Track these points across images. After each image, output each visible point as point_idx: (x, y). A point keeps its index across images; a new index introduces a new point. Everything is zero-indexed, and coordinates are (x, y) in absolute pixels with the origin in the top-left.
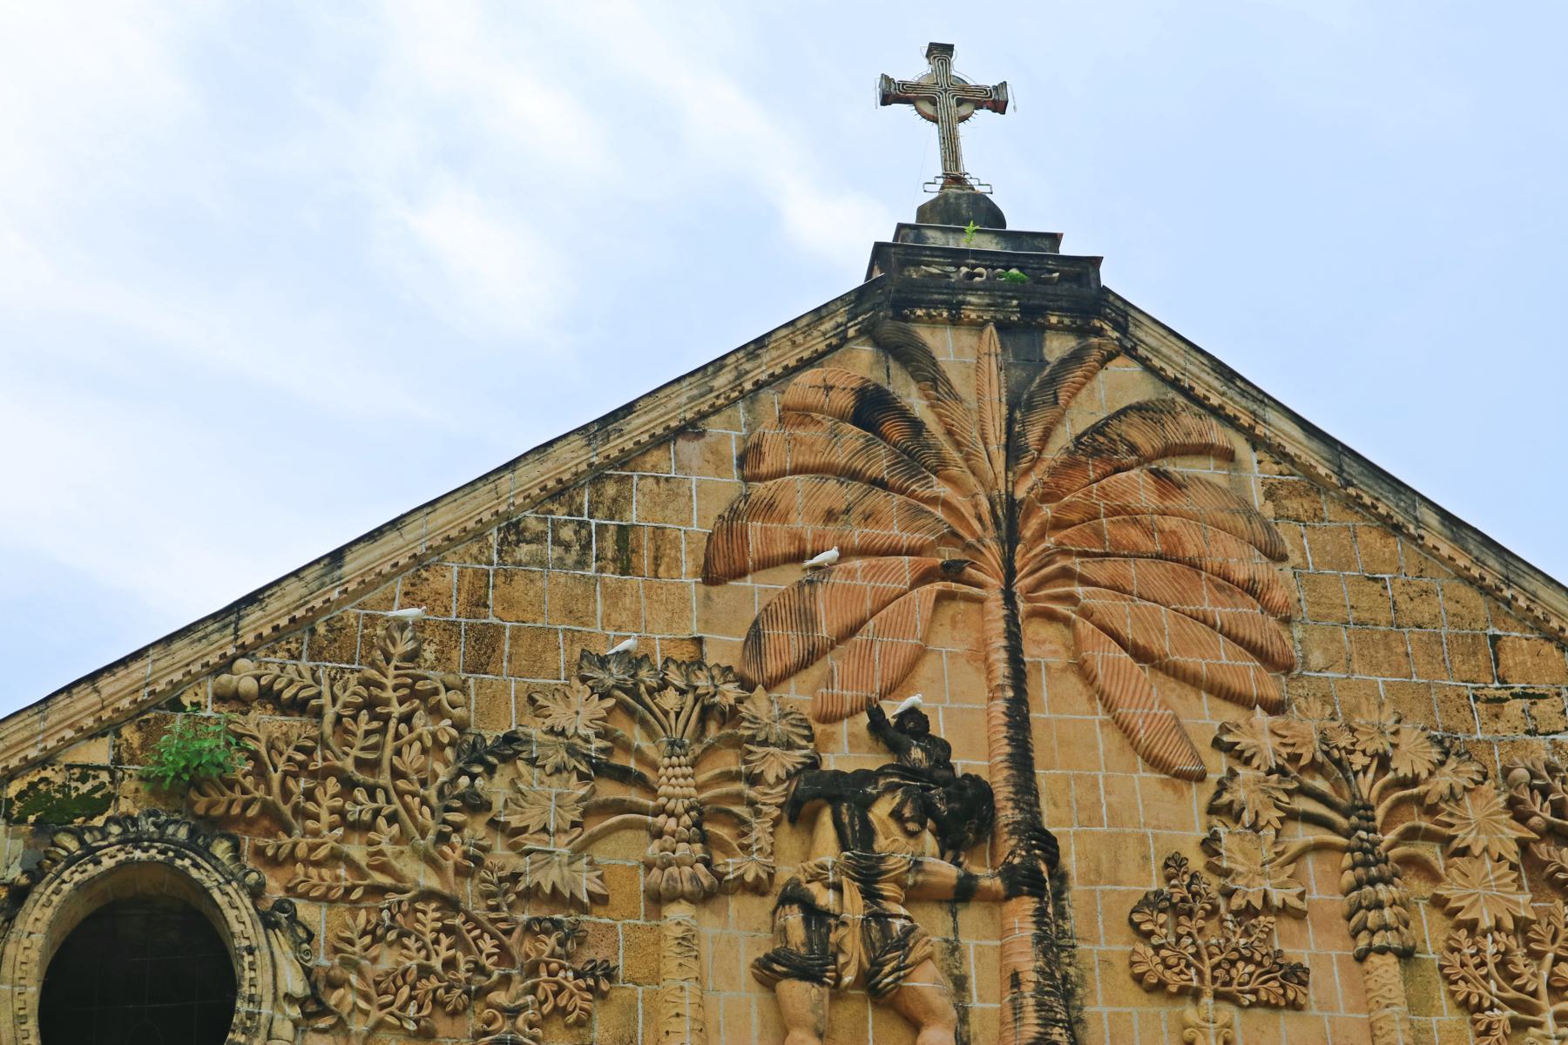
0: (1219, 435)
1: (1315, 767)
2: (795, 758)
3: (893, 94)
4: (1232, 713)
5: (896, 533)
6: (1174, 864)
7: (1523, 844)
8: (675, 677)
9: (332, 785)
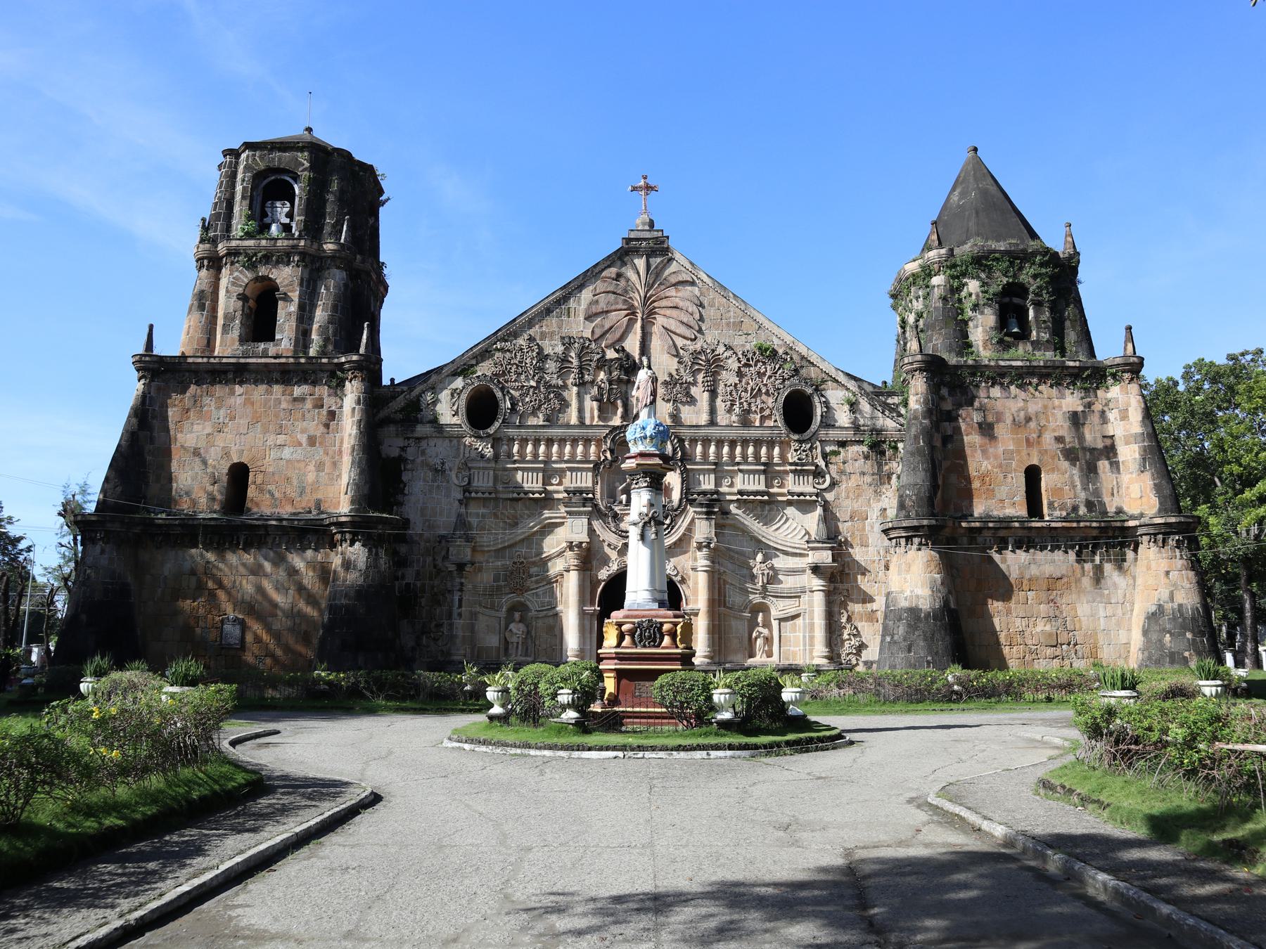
1: (700, 353)
2: (599, 356)
3: (634, 189)
5: (620, 306)
6: (671, 375)
7: (739, 367)
8: (577, 340)
9: (515, 366)
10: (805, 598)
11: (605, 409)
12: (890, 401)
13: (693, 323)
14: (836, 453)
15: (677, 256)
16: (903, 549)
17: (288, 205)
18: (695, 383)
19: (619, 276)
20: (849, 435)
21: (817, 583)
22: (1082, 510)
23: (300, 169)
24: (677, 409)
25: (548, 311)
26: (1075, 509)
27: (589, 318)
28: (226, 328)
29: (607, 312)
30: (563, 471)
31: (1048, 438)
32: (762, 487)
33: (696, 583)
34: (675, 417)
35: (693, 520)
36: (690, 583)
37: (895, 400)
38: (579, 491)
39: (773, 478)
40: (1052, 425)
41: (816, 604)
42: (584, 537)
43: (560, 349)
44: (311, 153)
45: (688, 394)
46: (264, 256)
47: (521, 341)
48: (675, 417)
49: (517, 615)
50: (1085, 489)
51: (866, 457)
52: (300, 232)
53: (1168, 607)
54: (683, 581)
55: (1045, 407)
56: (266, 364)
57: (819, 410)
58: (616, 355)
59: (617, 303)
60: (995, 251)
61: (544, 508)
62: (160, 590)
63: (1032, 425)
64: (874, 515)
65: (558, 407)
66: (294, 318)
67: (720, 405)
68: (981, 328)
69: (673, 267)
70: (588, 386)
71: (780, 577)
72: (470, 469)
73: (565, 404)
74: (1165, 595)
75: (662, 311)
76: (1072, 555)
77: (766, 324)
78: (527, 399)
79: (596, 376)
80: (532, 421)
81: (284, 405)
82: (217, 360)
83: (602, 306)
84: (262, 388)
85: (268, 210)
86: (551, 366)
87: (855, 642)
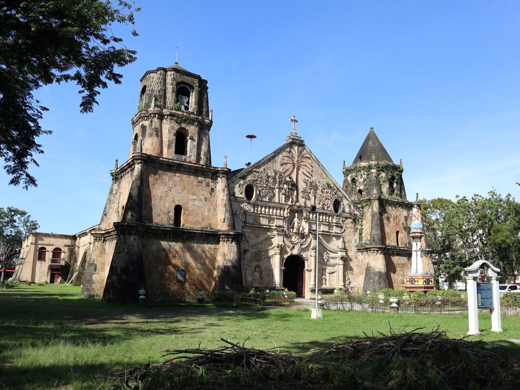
0: (310, 157)
4: (308, 178)
5: (291, 162)
10: (337, 267)
11: (287, 198)
12: (358, 206)
13: (310, 172)
14: (345, 221)
15: (306, 148)
16: (375, 254)
17: (187, 98)
18: (310, 193)
19: (290, 152)
20: (348, 215)
21: (341, 262)
22: (408, 245)
23: (195, 85)
24: (306, 201)
25: (269, 160)
26: (406, 244)
27: (282, 165)
28: (169, 147)
29: (286, 164)
30: (274, 219)
31: (401, 223)
32: (327, 230)
33: (311, 260)
34: (305, 203)
35: (311, 240)
36: (309, 260)
37: (359, 206)
38: (280, 227)
39: (331, 227)
40: (401, 219)
41: (340, 269)
42: (281, 243)
43: (273, 174)
44: (198, 80)
45: (309, 197)
46: (185, 119)
47: (261, 169)
48: (305, 203)
49: (257, 269)
50: (408, 239)
51: (352, 223)
52: (196, 112)
53: (429, 273)
54: (307, 260)
55: (400, 214)
56: (191, 166)
57: (342, 206)
58: (289, 180)
59: (290, 161)
60: (390, 165)
61: (268, 231)
62: (150, 257)
63: (397, 219)
64: (353, 241)
65: (272, 195)
66: (196, 147)
67: (317, 202)
68: (385, 188)
69: (305, 152)
70: (281, 189)
71: (330, 260)
72: (246, 215)
73: (274, 195)
74: (428, 270)
75: (302, 166)
76: (407, 258)
77: (329, 176)
78: (263, 191)
79: (284, 186)
80: (264, 199)
81: (195, 183)
82: (172, 161)
83: (285, 161)
84: (186, 176)
85: (180, 99)
86: (271, 180)
87: (348, 281)
